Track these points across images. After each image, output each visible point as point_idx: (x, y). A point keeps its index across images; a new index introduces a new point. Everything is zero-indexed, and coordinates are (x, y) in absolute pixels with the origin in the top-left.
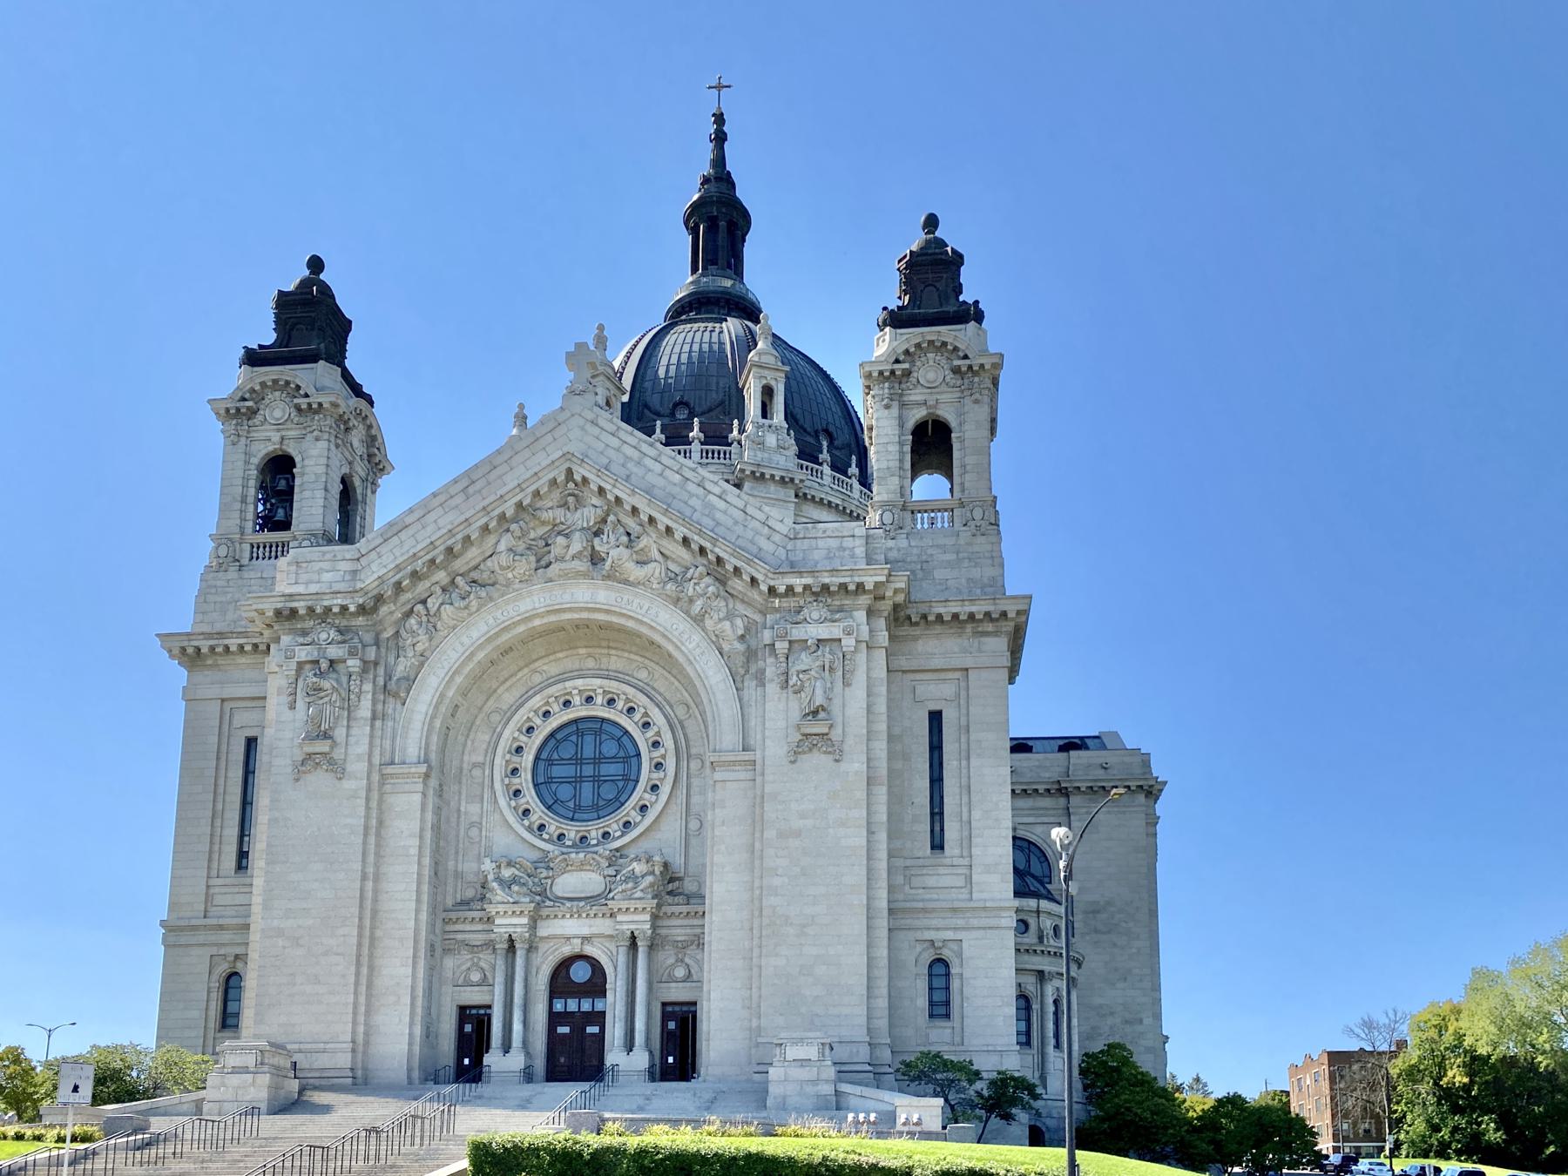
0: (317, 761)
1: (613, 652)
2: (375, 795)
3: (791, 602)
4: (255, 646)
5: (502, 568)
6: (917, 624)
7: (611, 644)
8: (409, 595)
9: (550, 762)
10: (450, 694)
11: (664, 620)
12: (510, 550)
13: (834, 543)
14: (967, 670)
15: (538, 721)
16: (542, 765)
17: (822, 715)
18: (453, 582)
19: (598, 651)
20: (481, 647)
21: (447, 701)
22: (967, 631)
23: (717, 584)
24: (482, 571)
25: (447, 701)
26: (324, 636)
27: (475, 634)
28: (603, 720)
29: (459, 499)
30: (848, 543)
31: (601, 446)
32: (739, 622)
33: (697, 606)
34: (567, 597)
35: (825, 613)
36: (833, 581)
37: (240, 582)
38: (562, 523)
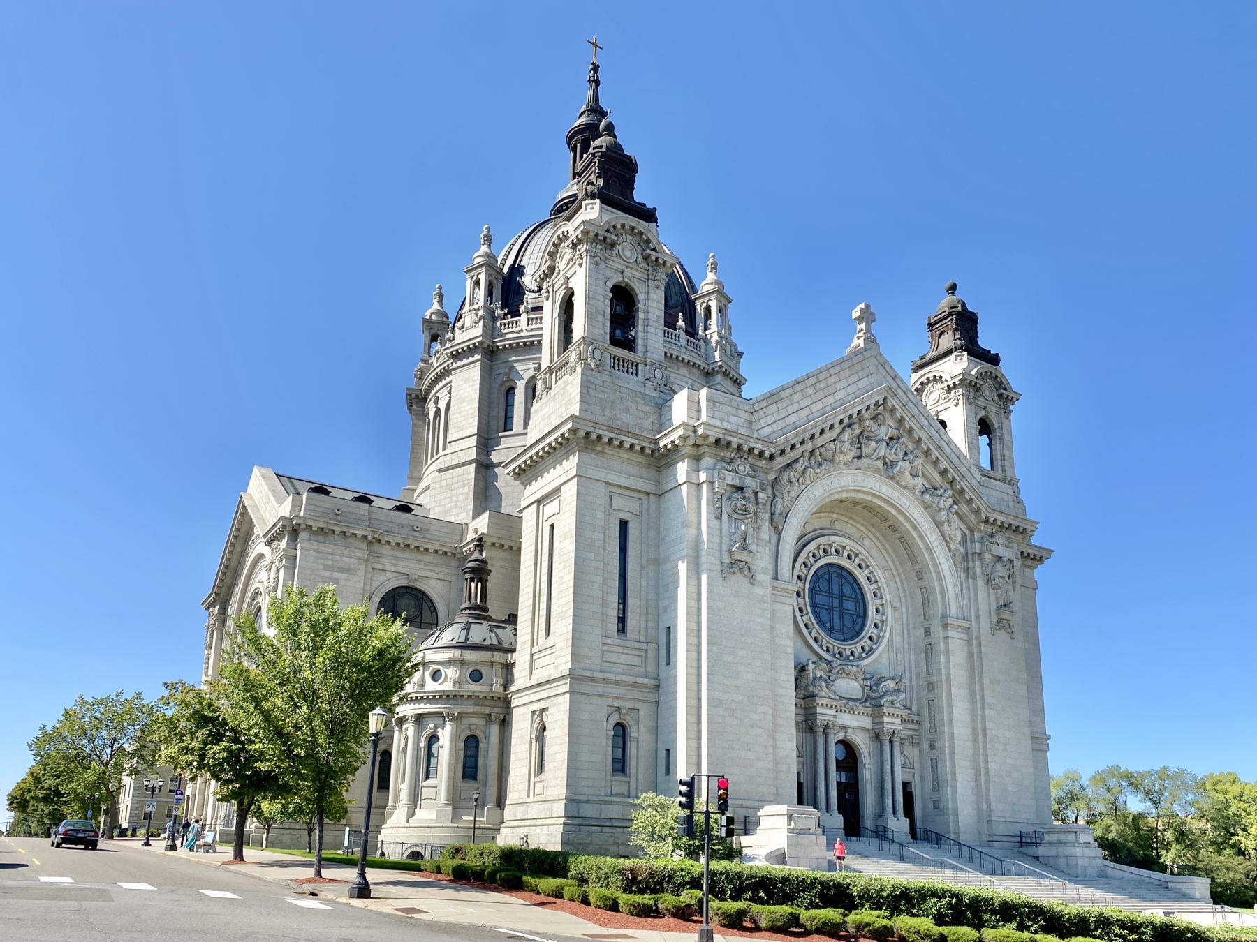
0: (741, 567)
1: (851, 522)
3: (988, 528)
4: (643, 448)
5: (841, 452)
7: (854, 517)
11: (920, 517)
19: (842, 518)
24: (827, 450)
27: (817, 494)
28: (843, 568)
29: (811, 391)
32: (959, 533)
33: (943, 516)
34: (866, 484)
36: (1015, 523)
37: (612, 385)
38: (871, 431)
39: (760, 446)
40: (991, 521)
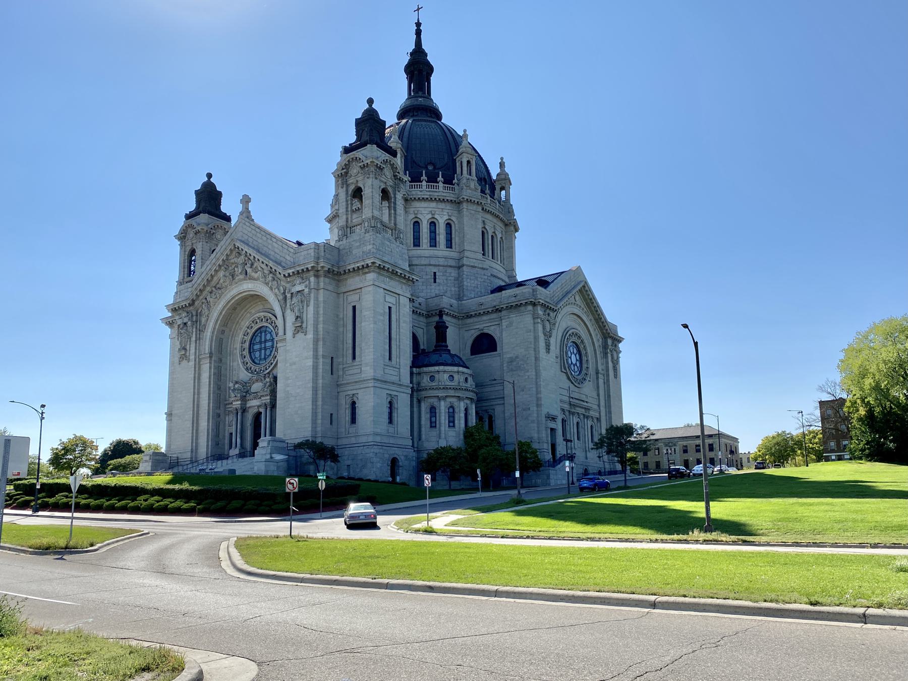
2: (197, 366)
6: (344, 274)
8: (201, 297)
9: (254, 344)
10: (217, 327)
12: (224, 276)
13: (306, 252)
14: (361, 288)
15: (249, 330)
16: (252, 345)
17: (299, 319)
18: (212, 290)
20: (223, 309)
21: (216, 330)
22: (361, 273)
23: (274, 276)
25: (216, 330)
26: (183, 315)
27: (220, 306)
30: (310, 251)
31: (246, 232)
32: (281, 288)
35: (300, 280)
36: (299, 269)
39: (185, 303)
40: (287, 275)
